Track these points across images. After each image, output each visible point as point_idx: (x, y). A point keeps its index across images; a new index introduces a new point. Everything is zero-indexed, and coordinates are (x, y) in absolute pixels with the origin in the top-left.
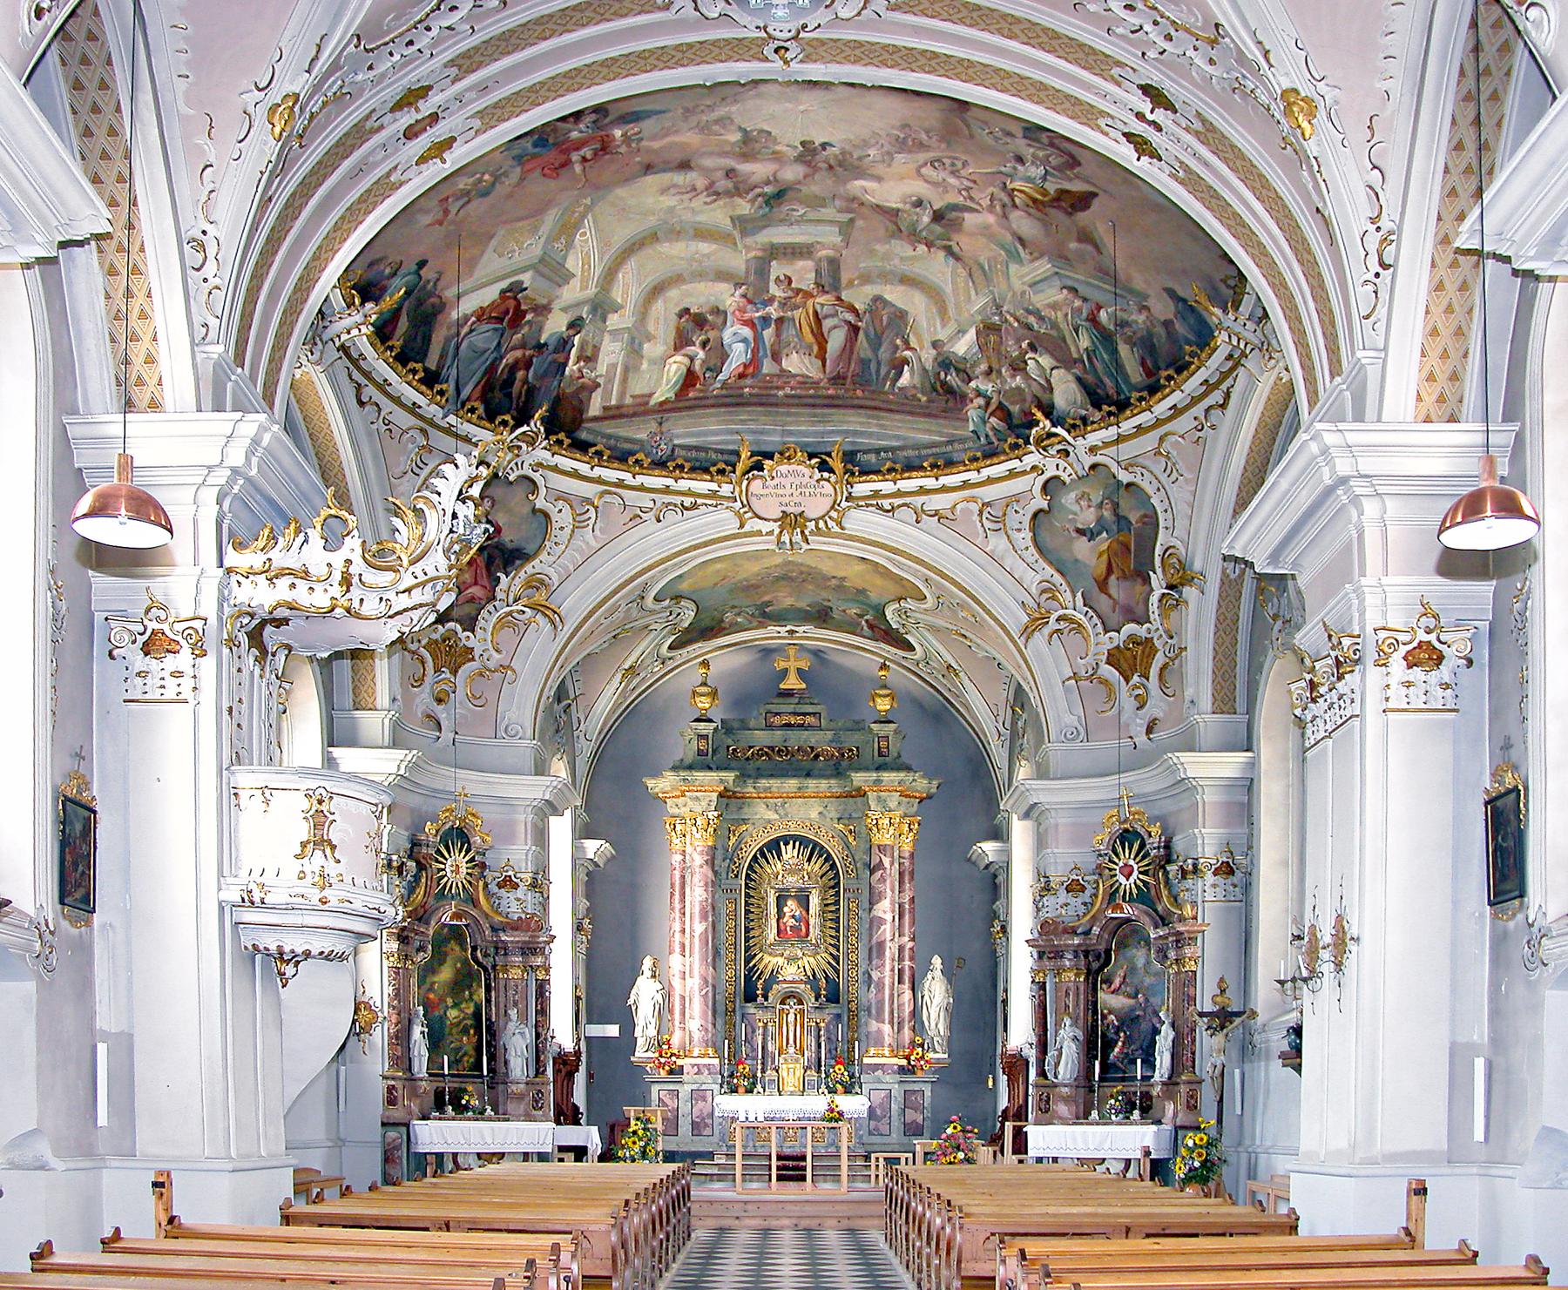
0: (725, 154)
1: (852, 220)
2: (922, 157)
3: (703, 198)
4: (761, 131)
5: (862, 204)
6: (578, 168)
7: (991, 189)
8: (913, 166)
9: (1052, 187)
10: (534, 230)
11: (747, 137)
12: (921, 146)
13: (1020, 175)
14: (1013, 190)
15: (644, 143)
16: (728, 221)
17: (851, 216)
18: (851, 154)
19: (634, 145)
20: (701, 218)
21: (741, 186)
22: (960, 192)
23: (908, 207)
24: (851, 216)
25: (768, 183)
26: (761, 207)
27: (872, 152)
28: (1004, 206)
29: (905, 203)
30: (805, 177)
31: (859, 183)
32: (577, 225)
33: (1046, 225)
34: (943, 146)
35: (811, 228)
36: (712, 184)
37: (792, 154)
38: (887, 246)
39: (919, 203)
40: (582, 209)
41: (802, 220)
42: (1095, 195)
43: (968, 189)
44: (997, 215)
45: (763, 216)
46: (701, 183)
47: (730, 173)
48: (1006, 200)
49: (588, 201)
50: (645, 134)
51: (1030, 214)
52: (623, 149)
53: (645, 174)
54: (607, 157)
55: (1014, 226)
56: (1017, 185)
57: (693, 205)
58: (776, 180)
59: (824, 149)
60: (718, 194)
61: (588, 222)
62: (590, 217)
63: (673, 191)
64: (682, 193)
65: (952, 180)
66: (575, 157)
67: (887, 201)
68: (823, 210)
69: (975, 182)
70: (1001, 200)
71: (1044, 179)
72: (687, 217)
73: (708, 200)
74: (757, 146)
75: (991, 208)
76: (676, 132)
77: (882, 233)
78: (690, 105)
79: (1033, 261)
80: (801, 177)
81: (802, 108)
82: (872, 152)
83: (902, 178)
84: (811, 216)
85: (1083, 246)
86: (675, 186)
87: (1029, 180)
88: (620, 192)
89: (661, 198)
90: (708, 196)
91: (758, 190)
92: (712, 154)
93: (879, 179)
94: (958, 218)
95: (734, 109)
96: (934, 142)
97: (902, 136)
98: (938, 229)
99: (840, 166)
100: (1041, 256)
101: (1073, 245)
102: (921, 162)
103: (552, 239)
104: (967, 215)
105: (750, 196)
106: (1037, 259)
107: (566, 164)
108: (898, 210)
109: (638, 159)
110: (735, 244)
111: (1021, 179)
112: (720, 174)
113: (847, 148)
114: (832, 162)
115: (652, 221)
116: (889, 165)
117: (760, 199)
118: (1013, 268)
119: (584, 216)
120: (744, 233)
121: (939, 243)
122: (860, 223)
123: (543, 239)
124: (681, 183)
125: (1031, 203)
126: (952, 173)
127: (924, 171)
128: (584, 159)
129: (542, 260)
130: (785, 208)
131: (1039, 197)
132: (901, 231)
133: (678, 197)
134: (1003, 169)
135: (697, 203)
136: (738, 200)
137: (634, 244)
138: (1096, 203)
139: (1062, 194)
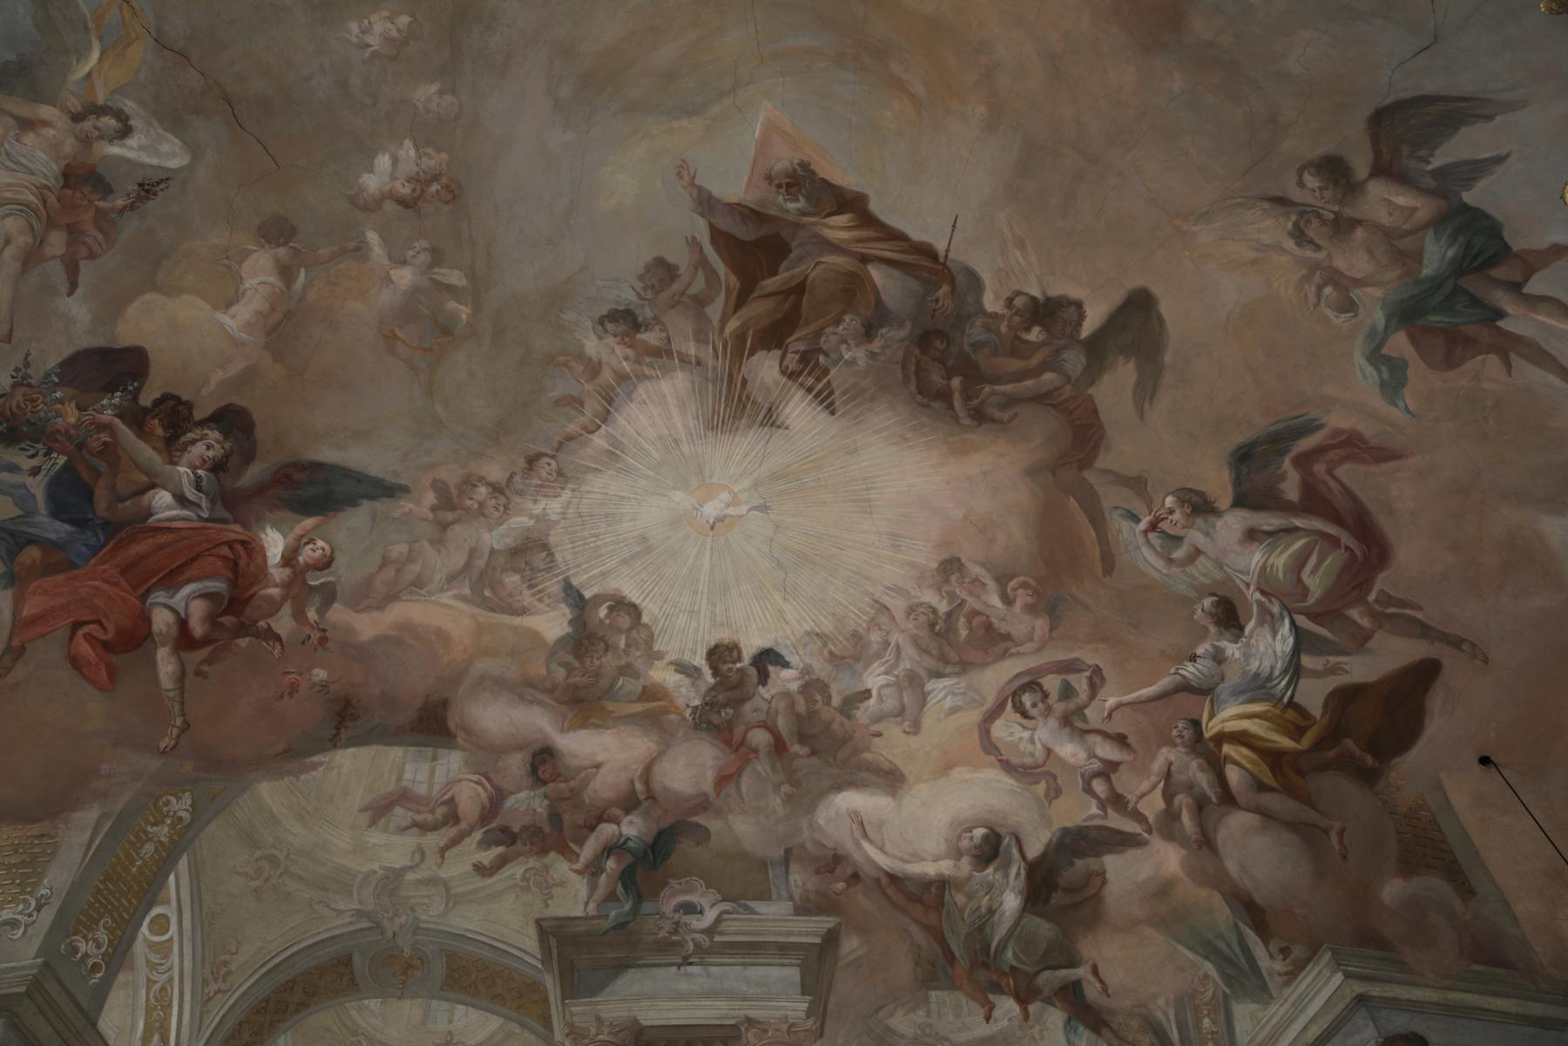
0: (525, 689)
1: (831, 939)
2: (995, 678)
3: (473, 852)
4: (621, 604)
5: (855, 877)
6: (166, 664)
7: (1165, 755)
8: (974, 716)
9: (1313, 695)
10: (29, 870)
11: (583, 639)
12: (993, 640)
13: (1233, 678)
14: (1221, 738)
15: (338, 613)
16: (530, 942)
17: (827, 922)
18: (824, 688)
19: (312, 614)
20: (468, 921)
21: (567, 818)
22: (1088, 790)
23: (965, 865)
24: (827, 922)
25: (630, 803)
26: (611, 897)
27: (875, 679)
28: (1200, 805)
29: (957, 854)
30: (722, 780)
31: (849, 800)
32: (149, 890)
33: (1308, 834)
34: (1041, 625)
35: (731, 975)
36: (498, 797)
37: (687, 694)
38: (920, 1016)
39: (990, 850)
40: (163, 832)
41: (715, 949)
42: (1425, 674)
43: (1108, 769)
44: (1183, 842)
45: (621, 926)
46: (470, 796)
47: (543, 760)
48: (1204, 781)
49: (181, 806)
50: (345, 573)
51: (1266, 815)
52: (283, 624)
53: (334, 742)
54: (243, 642)
55: (1232, 867)
56: (1229, 716)
57: (444, 874)
58: (651, 797)
59: (764, 678)
60: (507, 837)
61: (177, 883)
62: (183, 865)
63: (400, 815)
64: (424, 828)
65: (1069, 751)
66: (162, 620)
67: (918, 858)
68: (761, 907)
69: (1121, 740)
70: (1190, 787)
71: (1294, 669)
72: (432, 912)
73: (488, 856)
74: (609, 662)
75: (1168, 823)
76: (418, 583)
77: (903, 969)
78: (451, 475)
79: (1291, 976)
80: (708, 785)
81: (711, 510)
82: (875, 679)
83: (947, 768)
84: (737, 929)
85: (1418, 884)
86: (403, 797)
87: (1257, 687)
88: (268, 792)
89: (375, 838)
90: (486, 844)
91: (607, 830)
92: (499, 684)
93: (891, 780)
94: (1090, 875)
95: (553, 507)
96: (1018, 622)
97: (943, 607)
98: (1043, 929)
99: (803, 738)
100: (1314, 951)
101: (1392, 890)
102: (990, 702)
103: (71, 921)
104: (1112, 863)
105: (588, 850)
106: (1299, 967)
107: (136, 637)
108: (942, 883)
109: (320, 674)
110: (546, 1021)
111: (1236, 693)
112: (516, 764)
113: (820, 667)
114: (781, 723)
115: (338, 919)
116: (916, 728)
117: (611, 864)
118: (1245, 1014)
119: (165, 864)
120: (573, 986)
121: (1050, 979)
122: (850, 945)
123: (47, 916)
124: (421, 790)
125: (1268, 777)
126: (1066, 721)
127: (999, 730)
128: (184, 640)
129: (36, 984)
130: (669, 903)
131: (1286, 743)
132: (951, 958)
133: (411, 840)
134: (1190, 670)
135: (458, 867)
136: (561, 868)
137: (289, 986)
138: (1436, 701)
139: (1345, 698)
